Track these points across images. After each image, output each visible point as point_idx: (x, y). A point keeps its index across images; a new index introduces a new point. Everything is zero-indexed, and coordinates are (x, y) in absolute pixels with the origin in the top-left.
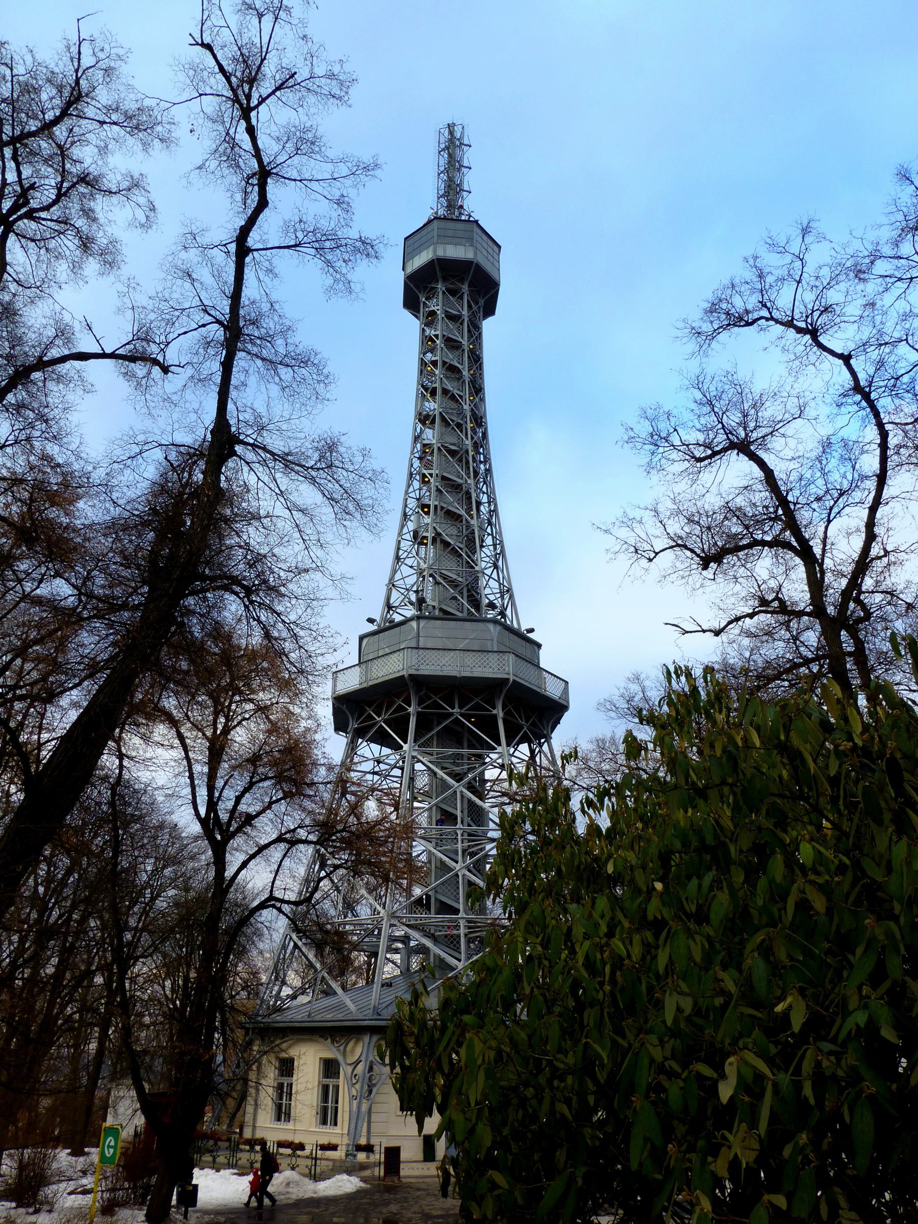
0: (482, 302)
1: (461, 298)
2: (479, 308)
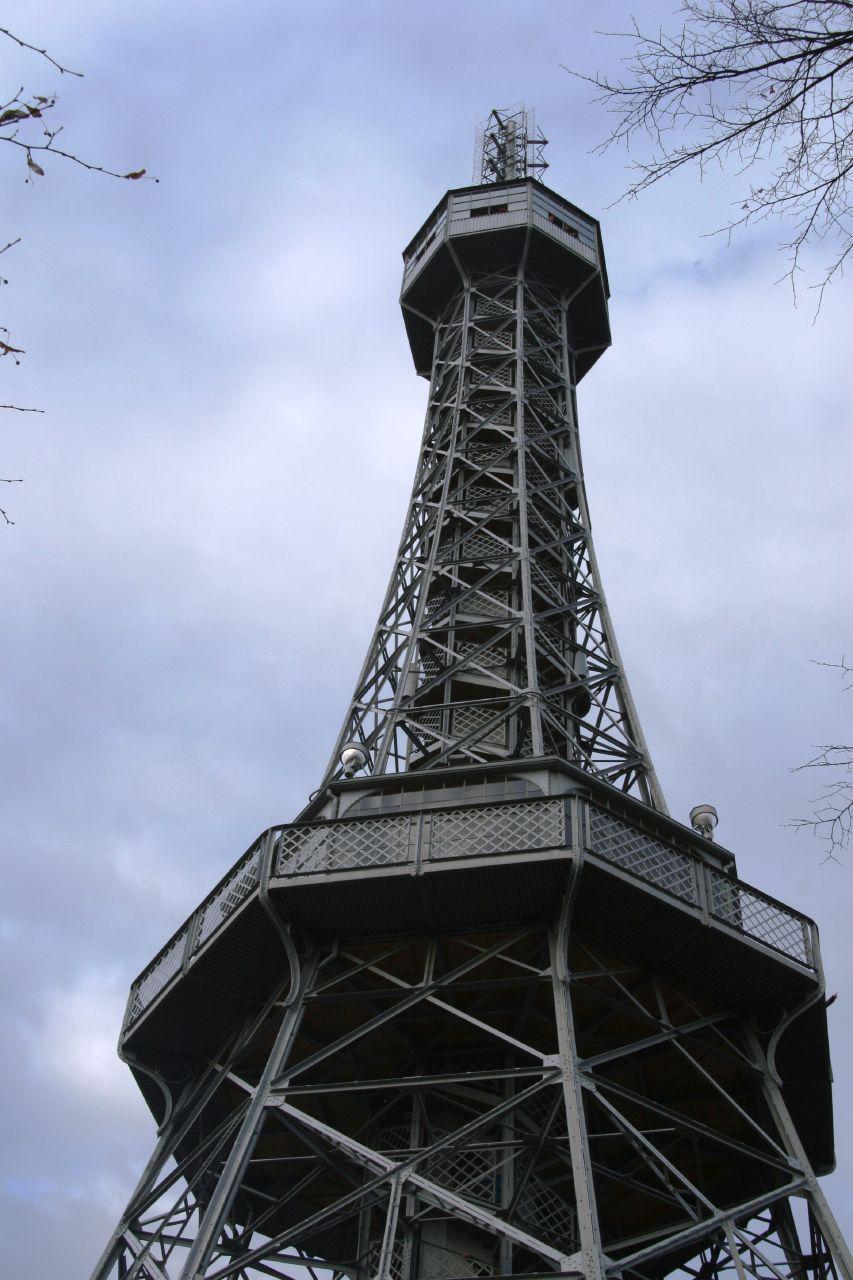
0: (565, 305)
1: (512, 295)
2: (558, 313)
